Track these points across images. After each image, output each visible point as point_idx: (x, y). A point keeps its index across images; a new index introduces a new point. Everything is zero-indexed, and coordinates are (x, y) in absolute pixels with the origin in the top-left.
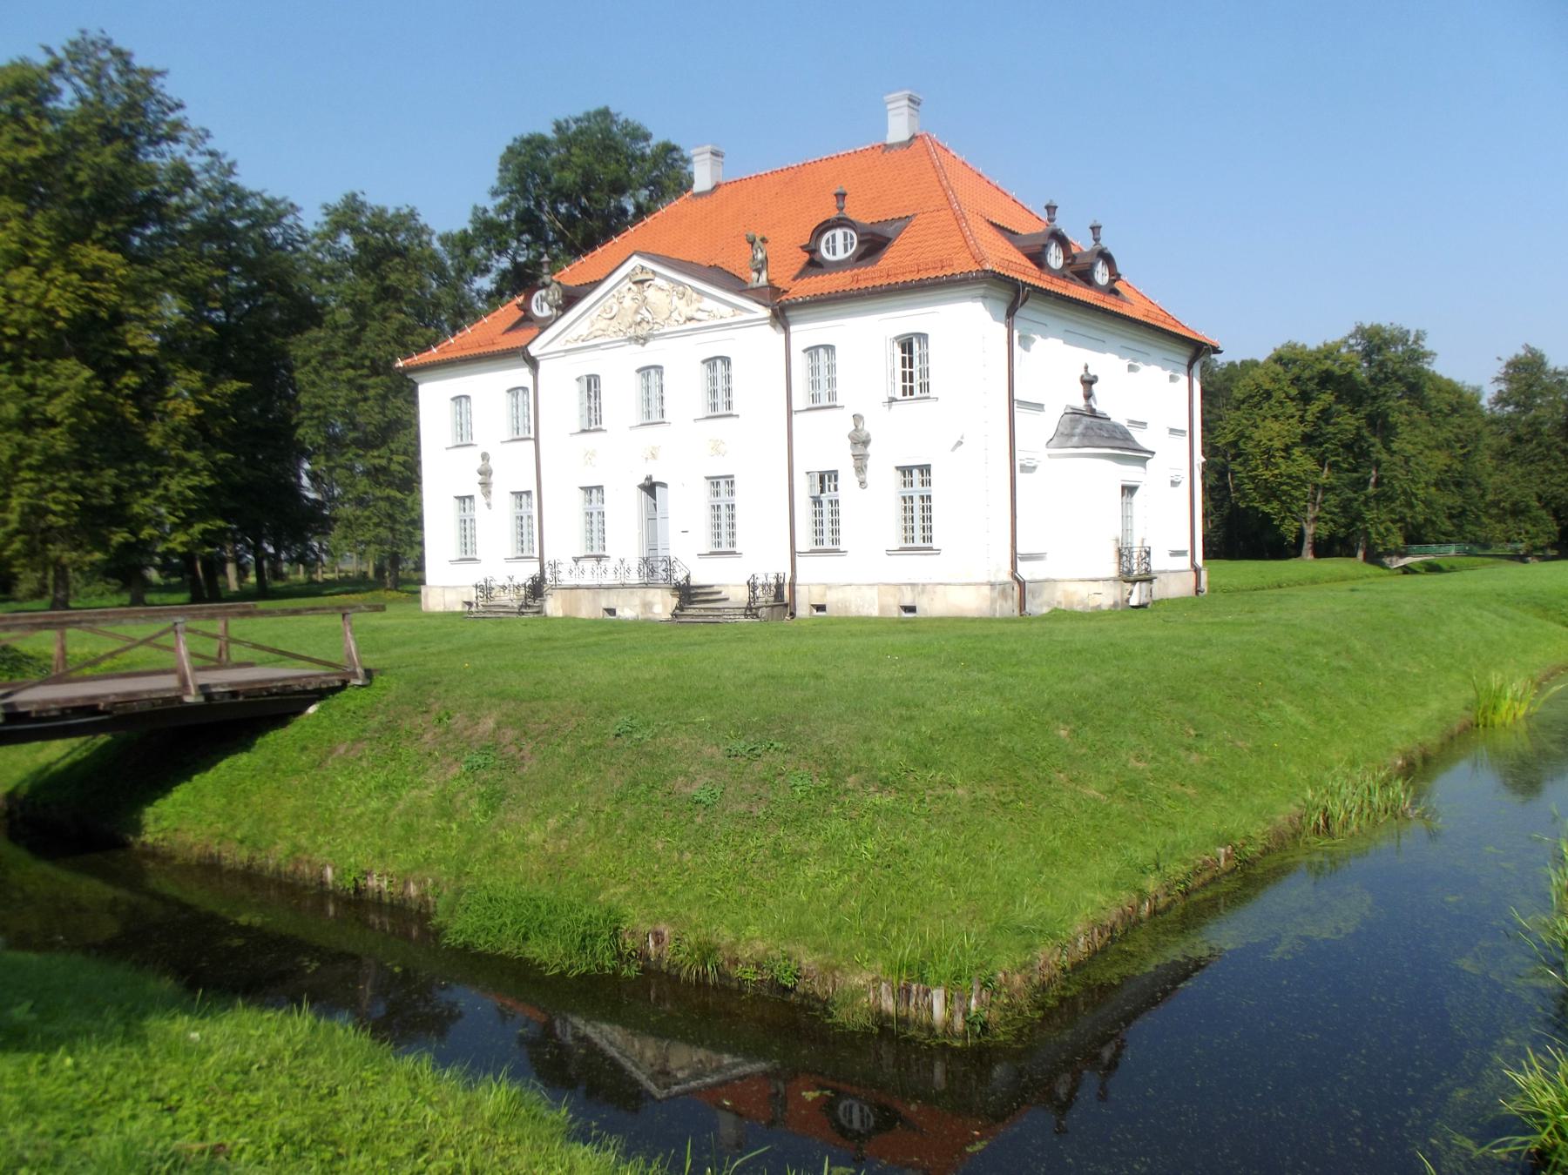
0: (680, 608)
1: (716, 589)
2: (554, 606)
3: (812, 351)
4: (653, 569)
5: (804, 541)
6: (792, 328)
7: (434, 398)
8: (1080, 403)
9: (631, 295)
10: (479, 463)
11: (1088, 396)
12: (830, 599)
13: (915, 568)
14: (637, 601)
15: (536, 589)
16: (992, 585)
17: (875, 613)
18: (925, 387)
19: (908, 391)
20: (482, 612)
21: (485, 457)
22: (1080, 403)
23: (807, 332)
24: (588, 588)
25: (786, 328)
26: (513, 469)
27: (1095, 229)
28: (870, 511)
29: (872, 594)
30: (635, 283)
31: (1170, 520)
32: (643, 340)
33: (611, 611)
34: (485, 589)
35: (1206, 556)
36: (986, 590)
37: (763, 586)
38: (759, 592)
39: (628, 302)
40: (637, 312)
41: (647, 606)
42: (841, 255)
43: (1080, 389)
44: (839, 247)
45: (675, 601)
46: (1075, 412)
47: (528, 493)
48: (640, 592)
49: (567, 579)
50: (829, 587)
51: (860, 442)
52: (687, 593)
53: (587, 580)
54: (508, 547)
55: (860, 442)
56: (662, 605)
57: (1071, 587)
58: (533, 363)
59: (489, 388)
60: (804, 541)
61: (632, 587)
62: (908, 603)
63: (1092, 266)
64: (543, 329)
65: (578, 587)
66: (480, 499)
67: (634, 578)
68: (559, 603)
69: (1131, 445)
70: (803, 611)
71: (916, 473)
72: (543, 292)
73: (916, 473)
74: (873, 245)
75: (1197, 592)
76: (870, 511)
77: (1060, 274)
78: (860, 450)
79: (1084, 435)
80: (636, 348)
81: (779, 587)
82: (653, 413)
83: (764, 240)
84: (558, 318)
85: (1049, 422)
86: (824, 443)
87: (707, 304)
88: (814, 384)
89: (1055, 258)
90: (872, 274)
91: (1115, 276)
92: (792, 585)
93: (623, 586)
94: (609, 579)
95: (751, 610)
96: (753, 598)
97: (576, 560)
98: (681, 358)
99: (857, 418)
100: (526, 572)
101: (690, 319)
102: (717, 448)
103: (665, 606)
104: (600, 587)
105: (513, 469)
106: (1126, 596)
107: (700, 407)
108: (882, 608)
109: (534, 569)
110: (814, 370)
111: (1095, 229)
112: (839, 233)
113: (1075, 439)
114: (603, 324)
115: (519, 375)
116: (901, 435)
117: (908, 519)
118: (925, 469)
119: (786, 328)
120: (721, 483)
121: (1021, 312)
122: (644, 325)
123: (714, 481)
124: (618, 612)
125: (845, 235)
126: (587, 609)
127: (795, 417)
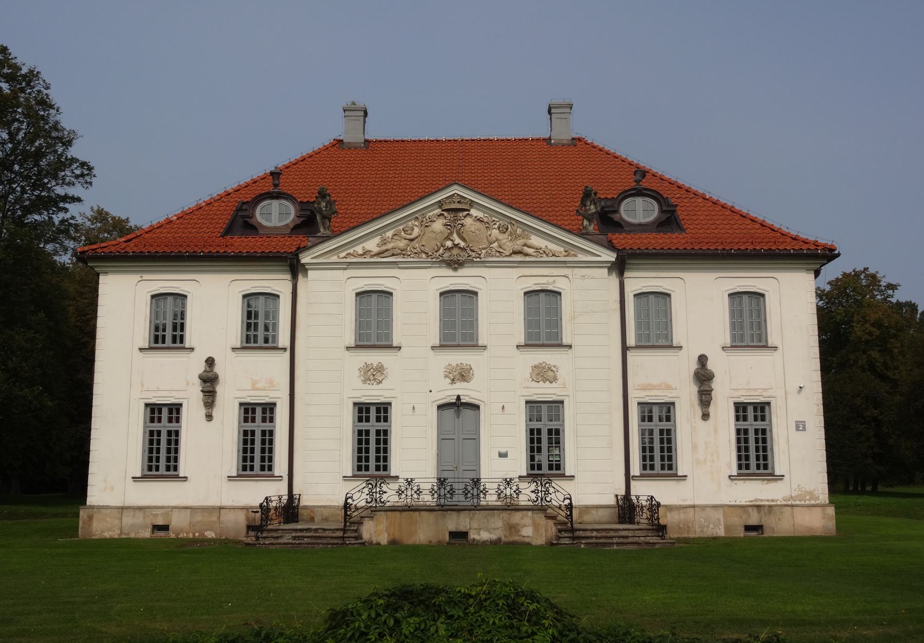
4: (458, 490)
5: (636, 469)
6: (626, 274)
13: (160, 494)
14: (499, 524)
17: (721, 532)
21: (210, 362)
23: (641, 280)
25: (621, 274)
26: (252, 376)
29: (719, 515)
32: (455, 264)
33: (459, 536)
41: (513, 528)
47: (269, 409)
48: (505, 515)
58: (296, 269)
62: (754, 520)
68: (382, 527)
80: (449, 272)
86: (663, 376)
87: (535, 241)
101: (515, 253)
102: (543, 373)
103: (536, 526)
108: (727, 528)
112: (639, 201)
116: (739, 376)
119: (621, 274)
124: (473, 535)
127: (629, 354)
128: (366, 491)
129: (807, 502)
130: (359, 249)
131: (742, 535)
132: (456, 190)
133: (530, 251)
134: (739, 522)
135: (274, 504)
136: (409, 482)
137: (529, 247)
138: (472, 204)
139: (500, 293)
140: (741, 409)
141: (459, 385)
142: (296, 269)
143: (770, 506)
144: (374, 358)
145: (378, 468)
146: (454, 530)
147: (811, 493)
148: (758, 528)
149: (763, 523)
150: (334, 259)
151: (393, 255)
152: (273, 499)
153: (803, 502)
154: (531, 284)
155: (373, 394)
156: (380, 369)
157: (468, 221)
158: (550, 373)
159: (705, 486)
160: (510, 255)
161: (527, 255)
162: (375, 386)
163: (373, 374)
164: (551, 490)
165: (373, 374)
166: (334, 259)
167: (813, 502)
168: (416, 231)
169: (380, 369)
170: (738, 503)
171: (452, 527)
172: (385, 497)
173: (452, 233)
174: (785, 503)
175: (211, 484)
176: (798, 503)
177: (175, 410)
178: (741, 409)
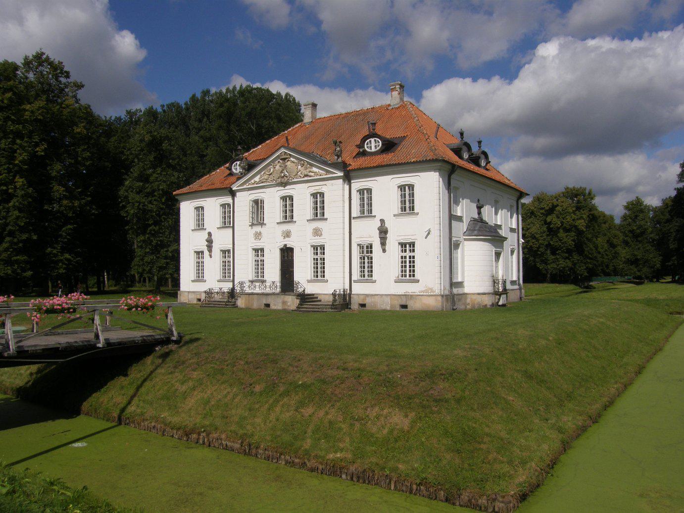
0: (301, 304)
1: (315, 296)
2: (241, 302)
3: (361, 192)
5: (355, 277)
7: (187, 209)
8: (476, 216)
9: (279, 164)
10: (207, 236)
11: (479, 213)
12: (368, 301)
15: (232, 293)
16: (442, 296)
17: (388, 308)
18: (412, 208)
19: (404, 209)
20: (209, 302)
21: (210, 234)
22: (476, 216)
24: (257, 294)
26: (222, 239)
27: (480, 142)
28: (386, 264)
29: (388, 300)
30: (281, 159)
31: (511, 268)
32: (284, 184)
33: (268, 305)
34: (209, 293)
35: (524, 282)
36: (440, 298)
37: (339, 295)
38: (337, 297)
39: (278, 167)
40: (282, 172)
41: (284, 303)
42: (373, 150)
43: (476, 210)
44: (373, 145)
45: (298, 301)
46: (475, 220)
47: (229, 251)
49: (247, 290)
50: (367, 295)
51: (383, 232)
52: (304, 298)
53: (257, 290)
54: (218, 275)
55: (383, 232)
56: (292, 302)
57: (474, 297)
58: (233, 194)
59: (212, 206)
60: (356, 276)
61: (278, 294)
62: (404, 303)
63: (479, 158)
64: (239, 179)
65: (252, 294)
66: (206, 253)
67: (278, 290)
68: (243, 301)
69: (498, 235)
70: (355, 306)
71: (408, 246)
72: (238, 163)
73: (408, 246)
74: (389, 146)
75: (521, 298)
76: (386, 264)
77: (467, 160)
78: (383, 235)
79: (479, 230)
80: (283, 188)
81: (344, 295)
82: (288, 216)
83: (340, 142)
84: (245, 175)
85: (464, 226)
86: (366, 231)
87: (315, 169)
88: (362, 205)
89: (466, 156)
90: (388, 158)
91: (488, 162)
92: (350, 294)
93: (274, 294)
94: (268, 290)
95: (333, 306)
96: (335, 300)
97: (252, 282)
98: (302, 194)
99: (382, 221)
100: (227, 286)
102: (317, 232)
104: (263, 294)
105: (222, 239)
106: (497, 301)
107: (309, 214)
108: (392, 306)
109: (230, 285)
110: (362, 199)
111: (480, 142)
113: (476, 232)
114: (266, 177)
115: (228, 200)
116: (401, 229)
117: (403, 267)
118: (412, 245)
120: (319, 249)
121: (453, 176)
122: (285, 178)
123: (315, 248)
124: (273, 307)
125: (375, 140)
126: (256, 304)
128: (239, 286)
129: (429, 294)
130: (253, 181)
131: (398, 309)
132: (283, 150)
133: (313, 174)
134: (397, 303)
135: (337, 293)
136: (273, 283)
137: (312, 172)
138: (290, 155)
139: (302, 194)
140: (403, 245)
141: (287, 239)
142: (233, 194)
143: (411, 295)
144: (258, 229)
145: (410, 276)
146: (266, 303)
147: (431, 289)
148: (404, 306)
149: (408, 304)
150: (245, 187)
151: (262, 182)
152: (337, 291)
153: (427, 294)
154: (313, 190)
155: (259, 245)
156: (260, 233)
157: (289, 163)
158: (319, 232)
159: (384, 285)
160: (304, 177)
161: (310, 176)
162: (259, 241)
163: (258, 236)
164: (299, 286)
165: (258, 236)
166: (245, 187)
167: (432, 294)
168: (272, 169)
169: (260, 233)
170: (398, 294)
171: (265, 302)
172: (245, 288)
173: (283, 170)
174: (419, 294)
175: (214, 281)
176: (425, 294)
177: (202, 252)
178: (403, 245)
